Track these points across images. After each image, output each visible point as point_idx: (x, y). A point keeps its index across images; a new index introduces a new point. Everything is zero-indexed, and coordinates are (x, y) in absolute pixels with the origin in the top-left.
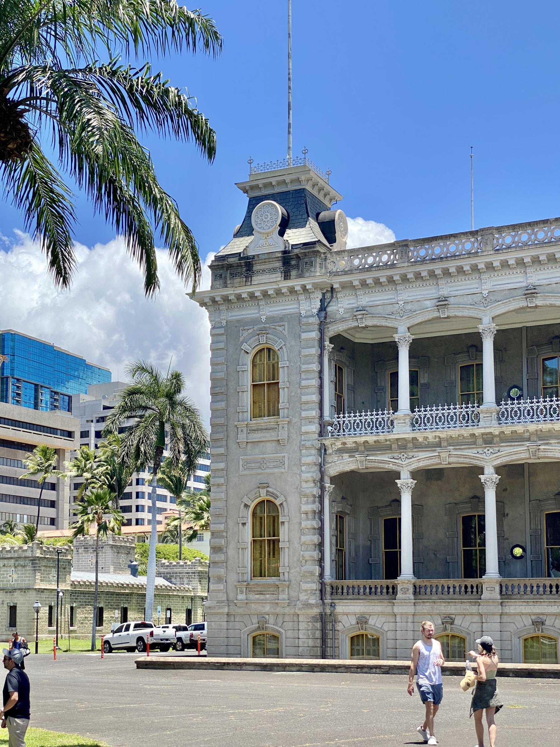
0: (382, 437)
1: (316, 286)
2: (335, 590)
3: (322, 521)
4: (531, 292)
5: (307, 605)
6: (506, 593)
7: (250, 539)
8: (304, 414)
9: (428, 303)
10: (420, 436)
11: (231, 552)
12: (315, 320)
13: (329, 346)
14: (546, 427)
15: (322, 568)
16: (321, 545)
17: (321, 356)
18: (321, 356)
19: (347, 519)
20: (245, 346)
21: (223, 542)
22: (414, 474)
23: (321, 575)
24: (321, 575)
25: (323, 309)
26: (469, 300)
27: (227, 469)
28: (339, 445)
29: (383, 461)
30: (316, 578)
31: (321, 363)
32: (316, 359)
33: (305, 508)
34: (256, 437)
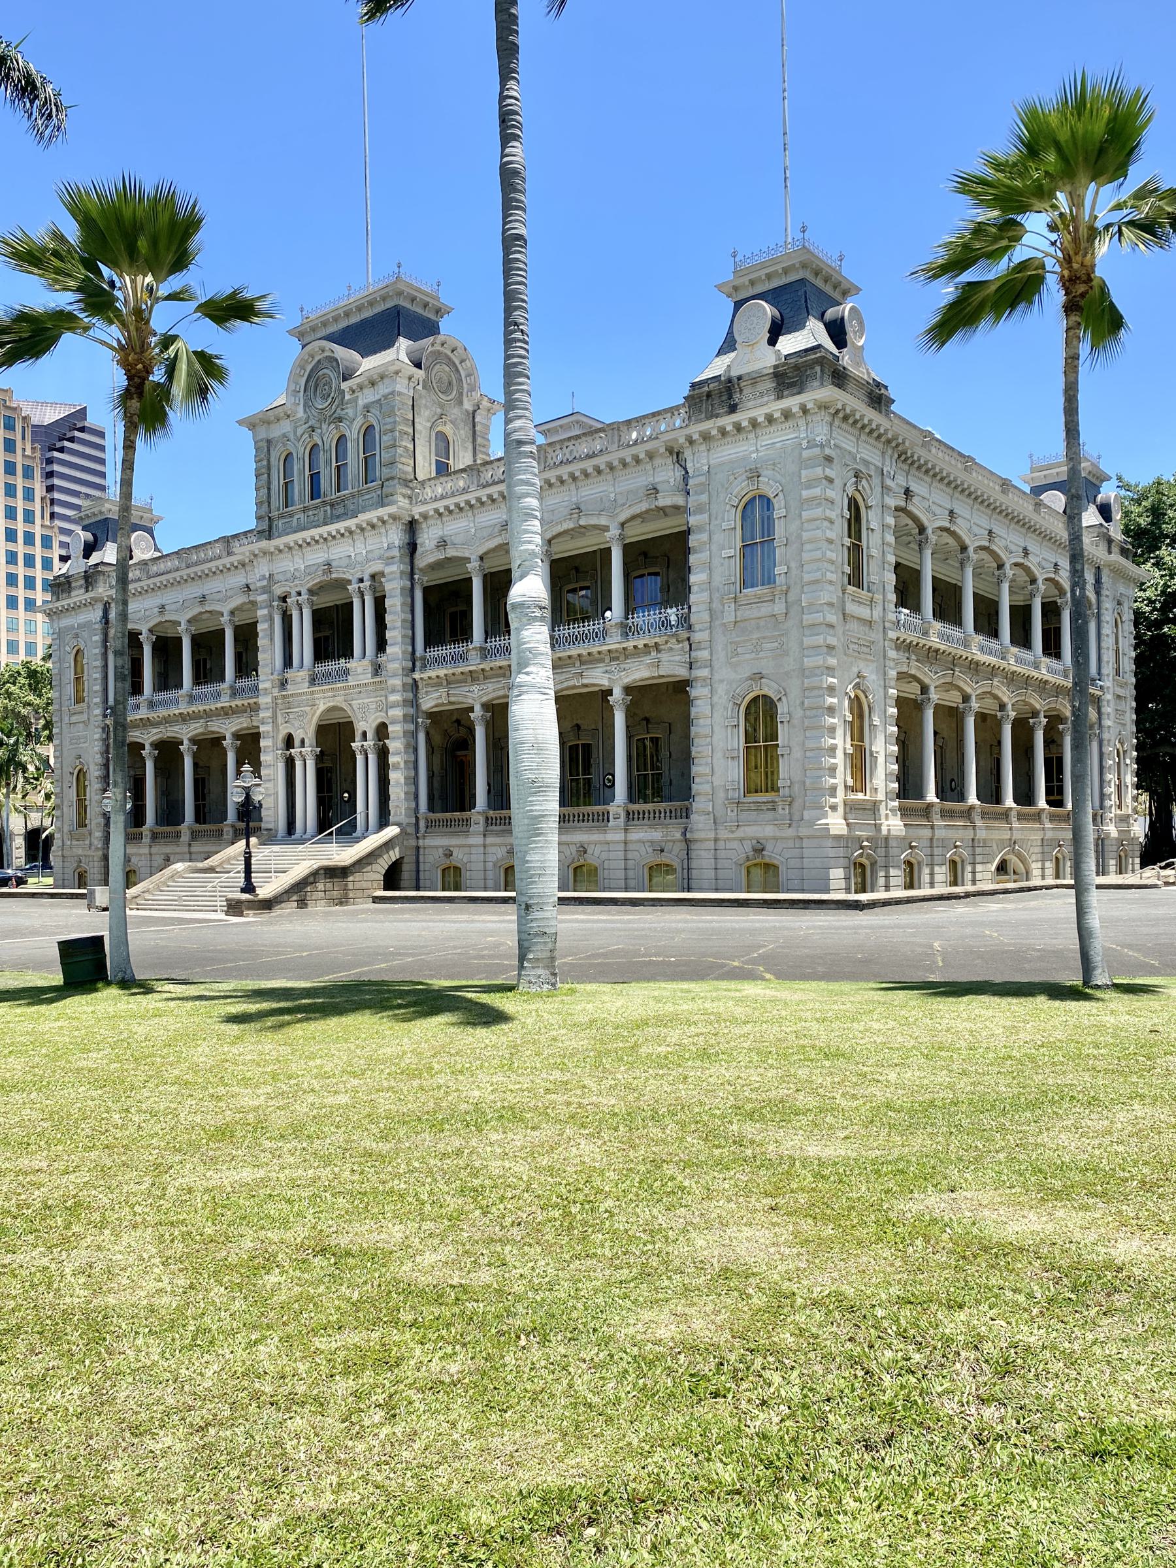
4: (203, 599)
5: (97, 849)
6: (155, 836)
26: (173, 607)
34: (74, 719)
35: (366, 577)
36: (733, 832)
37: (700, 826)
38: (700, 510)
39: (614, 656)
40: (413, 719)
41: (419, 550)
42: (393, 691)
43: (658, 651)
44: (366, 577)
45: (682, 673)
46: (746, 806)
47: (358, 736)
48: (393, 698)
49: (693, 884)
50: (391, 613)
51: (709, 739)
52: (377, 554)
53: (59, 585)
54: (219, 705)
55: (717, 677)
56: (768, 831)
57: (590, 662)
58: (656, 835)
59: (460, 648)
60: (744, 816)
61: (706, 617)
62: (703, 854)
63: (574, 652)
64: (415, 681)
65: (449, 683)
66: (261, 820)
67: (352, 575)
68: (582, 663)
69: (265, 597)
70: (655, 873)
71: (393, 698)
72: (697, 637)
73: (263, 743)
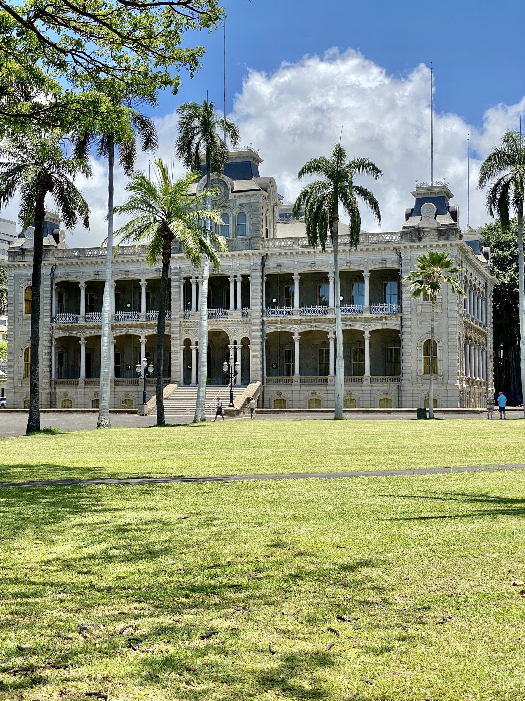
0: (74, 324)
1: (49, 264)
2: (56, 382)
3: (51, 356)
7: (23, 362)
8: (45, 314)
9: (92, 273)
10: (87, 324)
11: (16, 368)
12: (49, 277)
13: (55, 286)
14: (130, 323)
15: (51, 374)
16: (50, 366)
17: (51, 291)
18: (51, 291)
19: (64, 354)
20: (22, 285)
21: (12, 363)
22: (86, 339)
23: (51, 377)
24: (51, 377)
25: (52, 272)
27: (14, 334)
28: (58, 326)
29: (74, 333)
30: (49, 378)
31: (51, 294)
32: (49, 292)
33: (44, 351)
35: (239, 275)
39: (366, 320)
40: (262, 337)
41: (266, 267)
42: (255, 324)
44: (239, 275)
45: (397, 328)
47: (232, 342)
48: (254, 328)
50: (254, 292)
52: (246, 266)
53: (15, 252)
54: (138, 323)
55: (413, 331)
57: (354, 321)
59: (290, 309)
61: (409, 309)
62: (407, 395)
63: (349, 317)
64: (263, 321)
65: (281, 323)
66: (170, 376)
67: (231, 273)
68: (351, 321)
69: (178, 277)
70: (385, 402)
71: (254, 328)
72: (406, 316)
73: (172, 342)
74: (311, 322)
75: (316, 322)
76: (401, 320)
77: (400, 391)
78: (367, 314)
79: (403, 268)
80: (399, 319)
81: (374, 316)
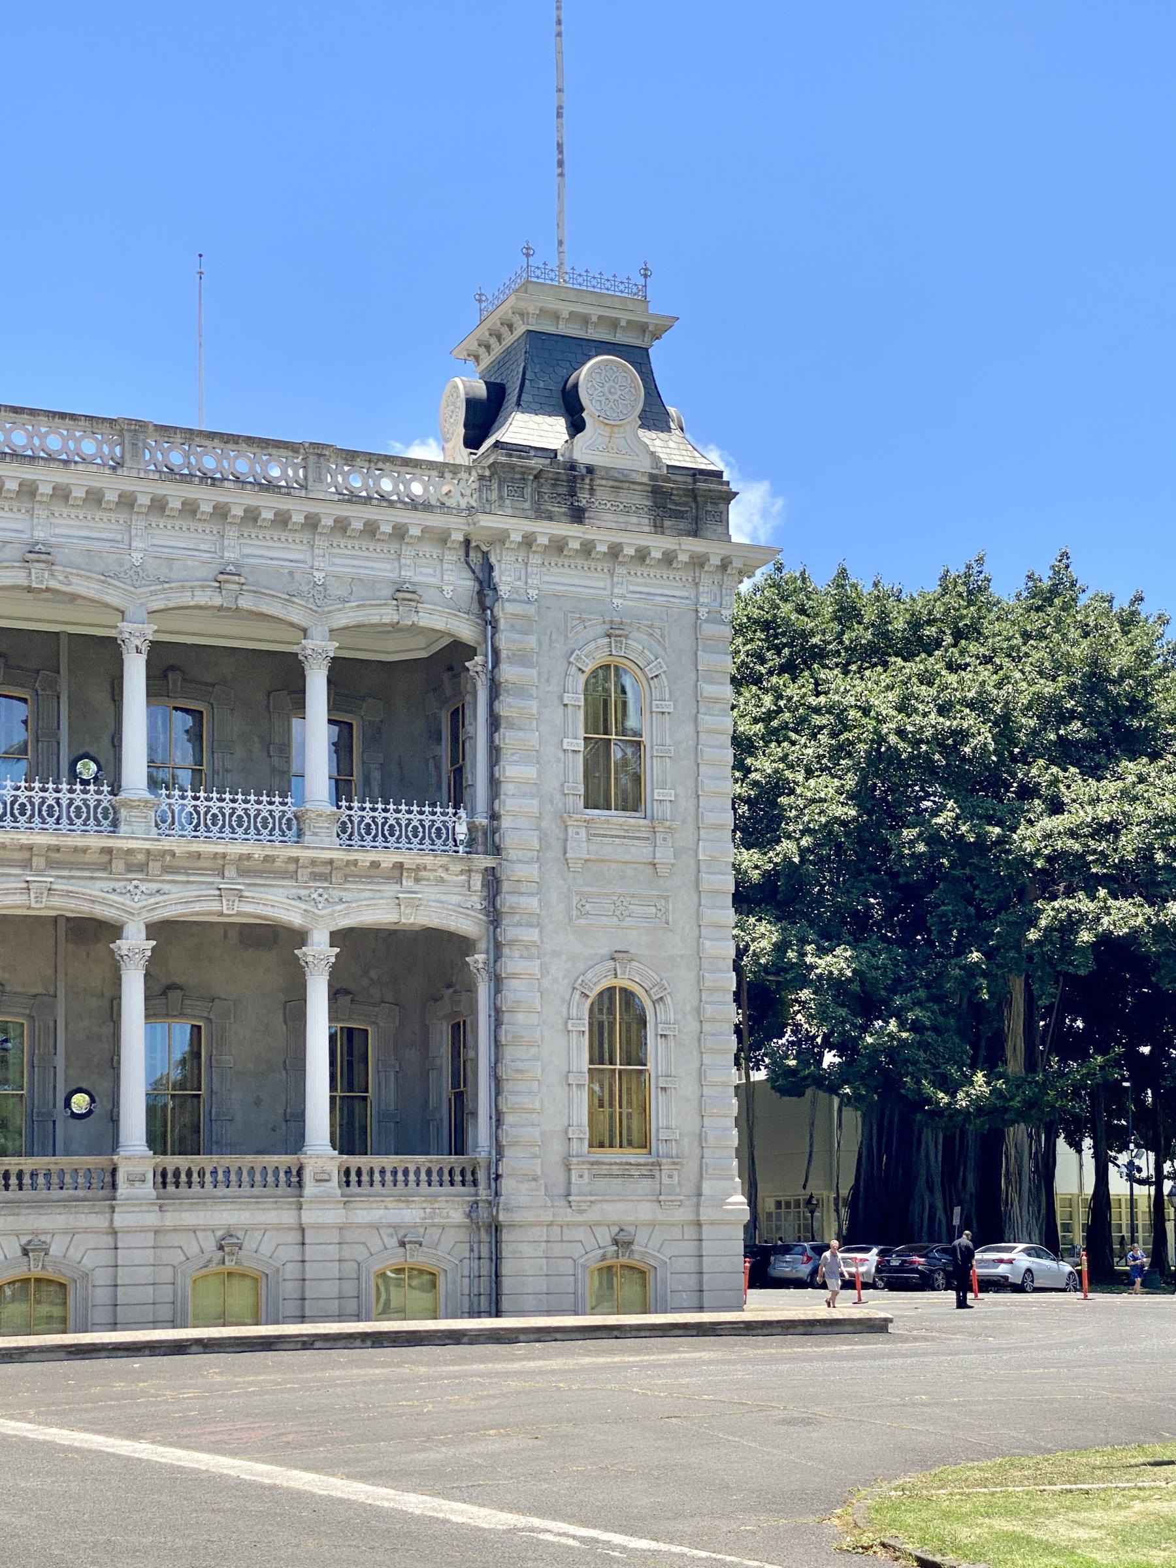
36: (581, 1212)
37: (524, 1200)
38: (522, 658)
39: (325, 872)
43: (417, 880)
45: (467, 924)
46: (604, 1169)
49: (505, 1305)
51: (534, 1050)
56: (645, 1211)
57: (258, 873)
58: (410, 1214)
60: (601, 1183)
62: (527, 1249)
63: (236, 849)
68: (242, 873)
74: (27, 864)
75: (51, 864)
76: (493, 883)
77: (491, 1230)
78: (322, 845)
79: (505, 642)
80: (477, 881)
81: (366, 858)
